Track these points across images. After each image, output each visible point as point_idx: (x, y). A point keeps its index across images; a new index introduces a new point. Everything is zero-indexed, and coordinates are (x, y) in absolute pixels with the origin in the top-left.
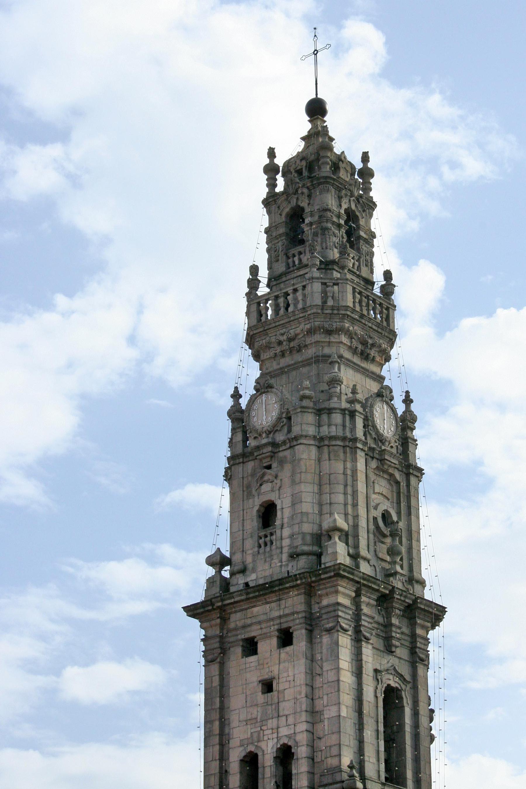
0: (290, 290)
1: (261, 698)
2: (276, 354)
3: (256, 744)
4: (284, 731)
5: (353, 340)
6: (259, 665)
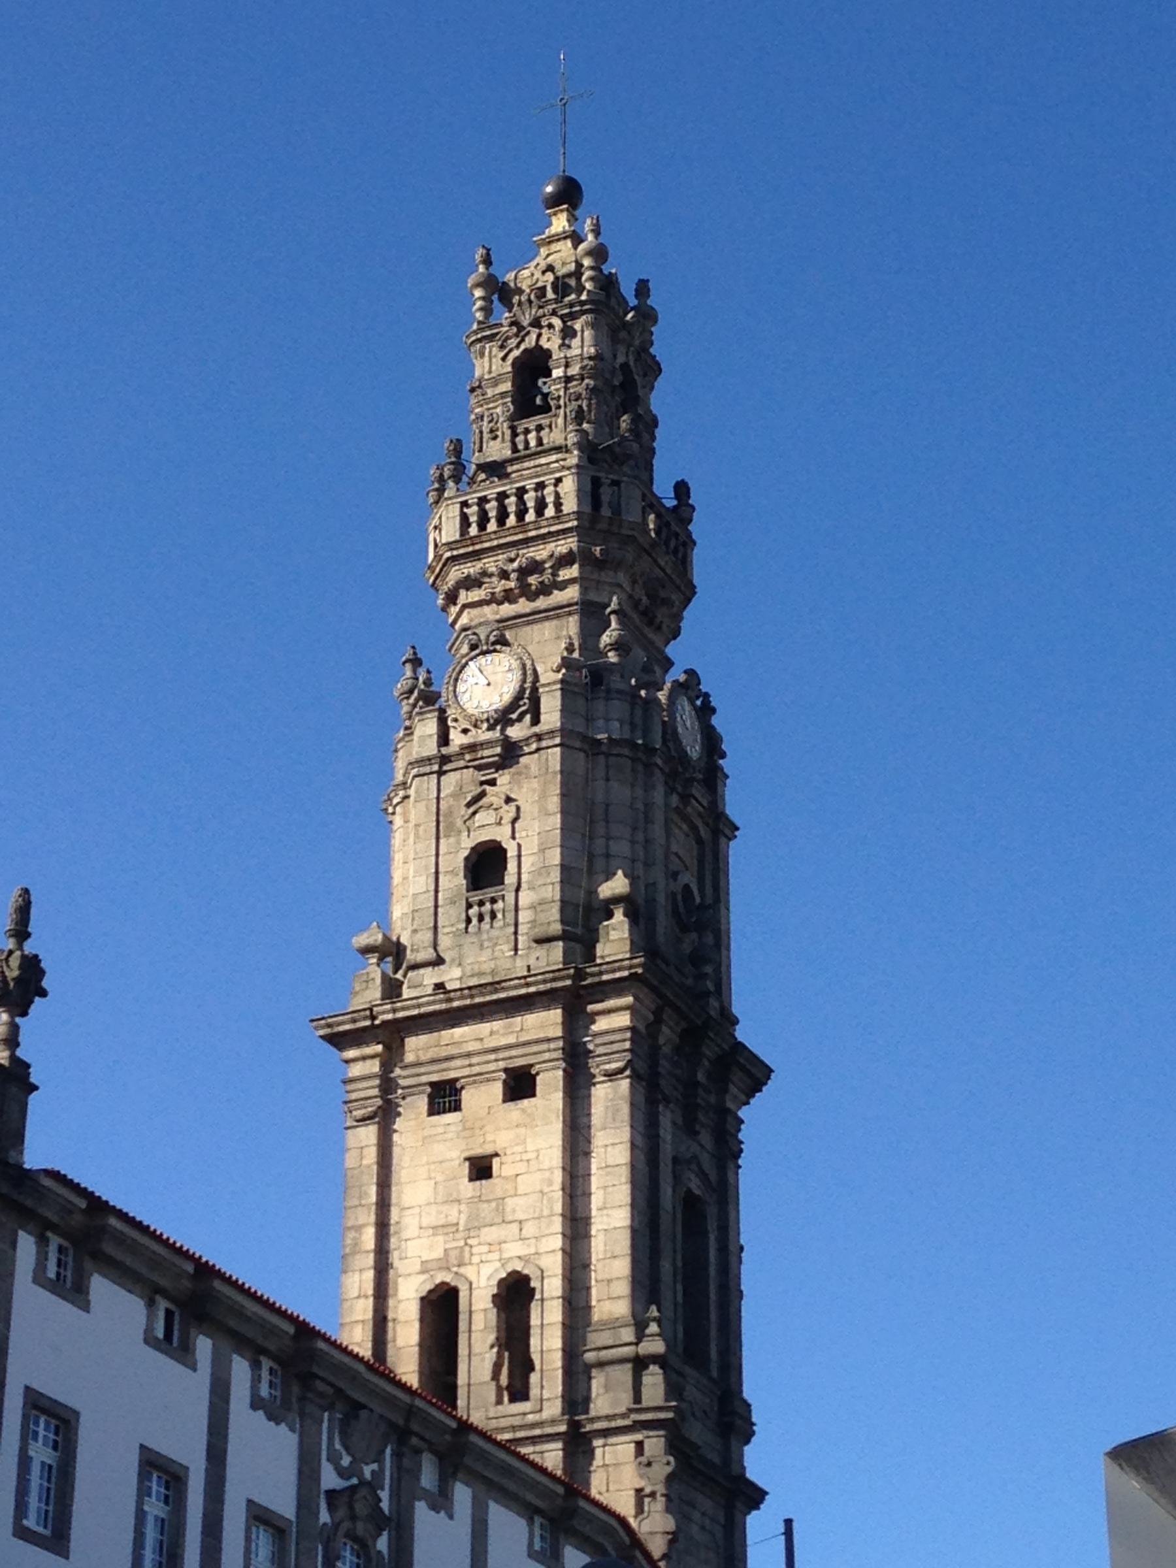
0: (530, 484)
1: (468, 1189)
2: (493, 594)
3: (455, 1269)
4: (514, 1249)
6: (465, 1129)
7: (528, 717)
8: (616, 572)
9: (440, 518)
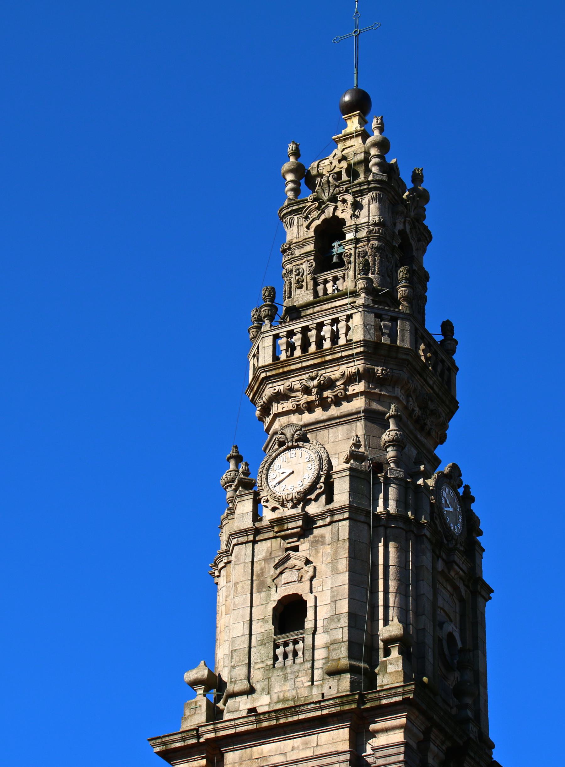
0: (327, 320)
2: (298, 405)
5: (410, 398)
7: (323, 497)
8: (394, 387)
9: (258, 348)
